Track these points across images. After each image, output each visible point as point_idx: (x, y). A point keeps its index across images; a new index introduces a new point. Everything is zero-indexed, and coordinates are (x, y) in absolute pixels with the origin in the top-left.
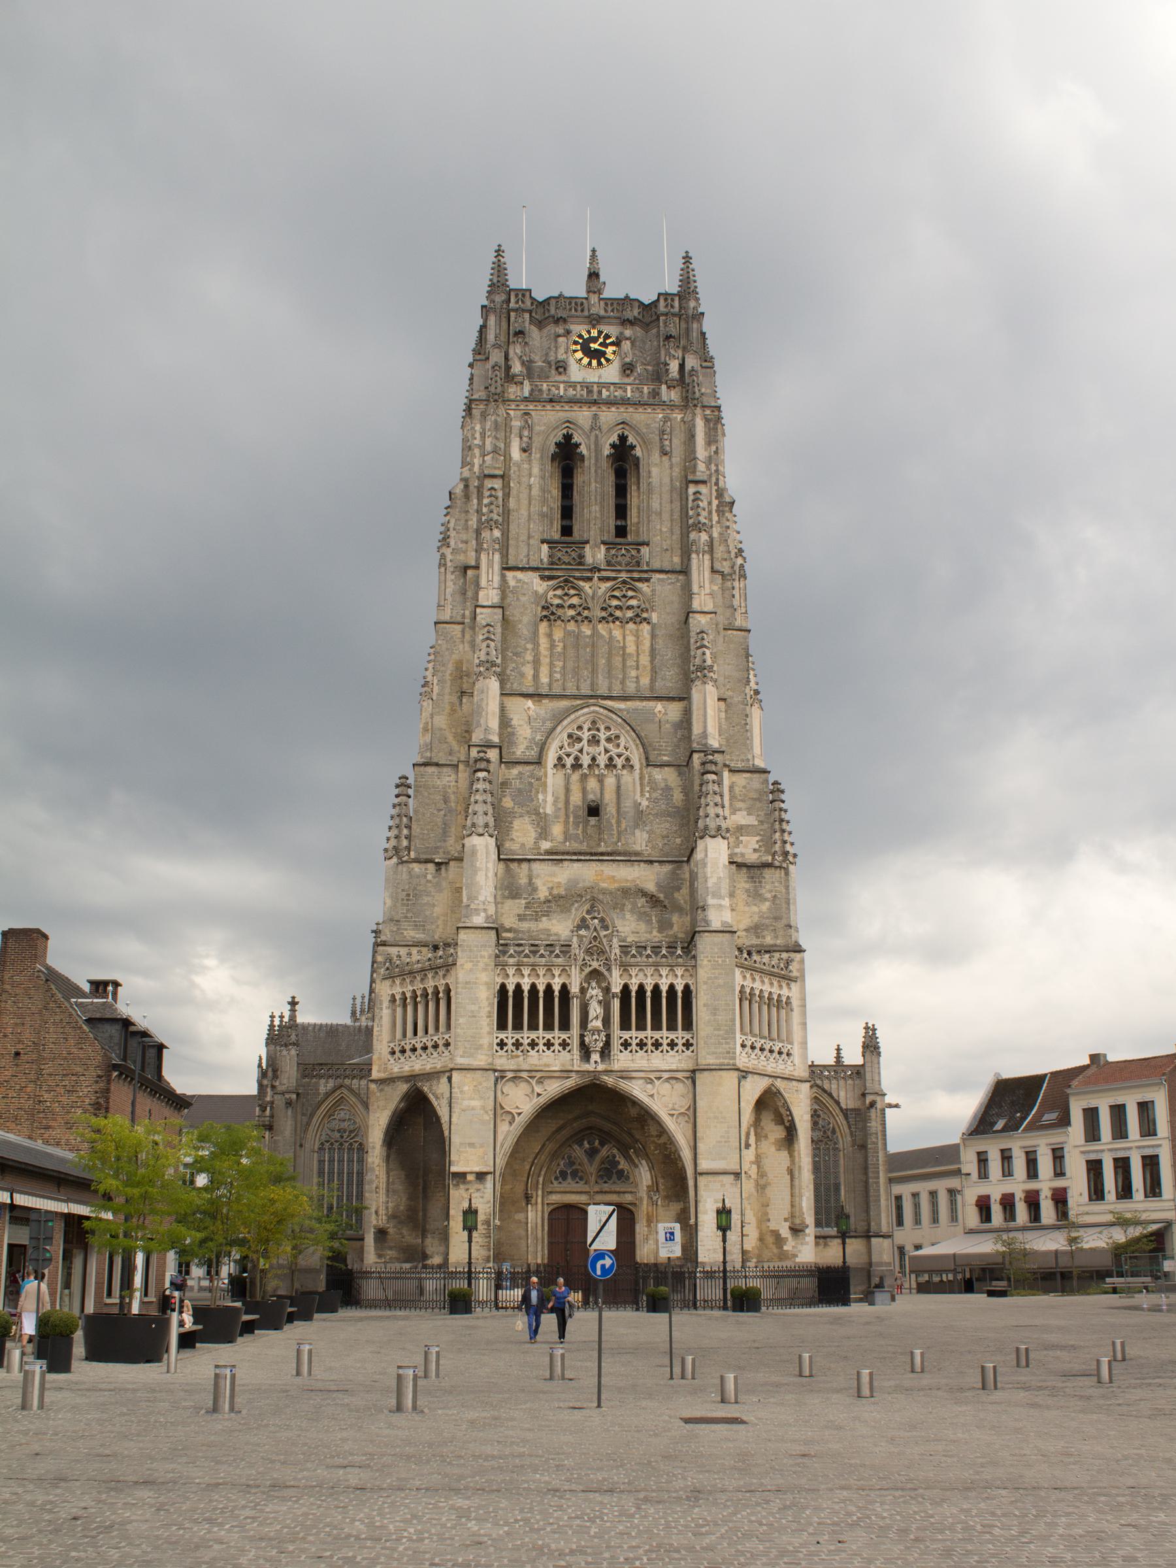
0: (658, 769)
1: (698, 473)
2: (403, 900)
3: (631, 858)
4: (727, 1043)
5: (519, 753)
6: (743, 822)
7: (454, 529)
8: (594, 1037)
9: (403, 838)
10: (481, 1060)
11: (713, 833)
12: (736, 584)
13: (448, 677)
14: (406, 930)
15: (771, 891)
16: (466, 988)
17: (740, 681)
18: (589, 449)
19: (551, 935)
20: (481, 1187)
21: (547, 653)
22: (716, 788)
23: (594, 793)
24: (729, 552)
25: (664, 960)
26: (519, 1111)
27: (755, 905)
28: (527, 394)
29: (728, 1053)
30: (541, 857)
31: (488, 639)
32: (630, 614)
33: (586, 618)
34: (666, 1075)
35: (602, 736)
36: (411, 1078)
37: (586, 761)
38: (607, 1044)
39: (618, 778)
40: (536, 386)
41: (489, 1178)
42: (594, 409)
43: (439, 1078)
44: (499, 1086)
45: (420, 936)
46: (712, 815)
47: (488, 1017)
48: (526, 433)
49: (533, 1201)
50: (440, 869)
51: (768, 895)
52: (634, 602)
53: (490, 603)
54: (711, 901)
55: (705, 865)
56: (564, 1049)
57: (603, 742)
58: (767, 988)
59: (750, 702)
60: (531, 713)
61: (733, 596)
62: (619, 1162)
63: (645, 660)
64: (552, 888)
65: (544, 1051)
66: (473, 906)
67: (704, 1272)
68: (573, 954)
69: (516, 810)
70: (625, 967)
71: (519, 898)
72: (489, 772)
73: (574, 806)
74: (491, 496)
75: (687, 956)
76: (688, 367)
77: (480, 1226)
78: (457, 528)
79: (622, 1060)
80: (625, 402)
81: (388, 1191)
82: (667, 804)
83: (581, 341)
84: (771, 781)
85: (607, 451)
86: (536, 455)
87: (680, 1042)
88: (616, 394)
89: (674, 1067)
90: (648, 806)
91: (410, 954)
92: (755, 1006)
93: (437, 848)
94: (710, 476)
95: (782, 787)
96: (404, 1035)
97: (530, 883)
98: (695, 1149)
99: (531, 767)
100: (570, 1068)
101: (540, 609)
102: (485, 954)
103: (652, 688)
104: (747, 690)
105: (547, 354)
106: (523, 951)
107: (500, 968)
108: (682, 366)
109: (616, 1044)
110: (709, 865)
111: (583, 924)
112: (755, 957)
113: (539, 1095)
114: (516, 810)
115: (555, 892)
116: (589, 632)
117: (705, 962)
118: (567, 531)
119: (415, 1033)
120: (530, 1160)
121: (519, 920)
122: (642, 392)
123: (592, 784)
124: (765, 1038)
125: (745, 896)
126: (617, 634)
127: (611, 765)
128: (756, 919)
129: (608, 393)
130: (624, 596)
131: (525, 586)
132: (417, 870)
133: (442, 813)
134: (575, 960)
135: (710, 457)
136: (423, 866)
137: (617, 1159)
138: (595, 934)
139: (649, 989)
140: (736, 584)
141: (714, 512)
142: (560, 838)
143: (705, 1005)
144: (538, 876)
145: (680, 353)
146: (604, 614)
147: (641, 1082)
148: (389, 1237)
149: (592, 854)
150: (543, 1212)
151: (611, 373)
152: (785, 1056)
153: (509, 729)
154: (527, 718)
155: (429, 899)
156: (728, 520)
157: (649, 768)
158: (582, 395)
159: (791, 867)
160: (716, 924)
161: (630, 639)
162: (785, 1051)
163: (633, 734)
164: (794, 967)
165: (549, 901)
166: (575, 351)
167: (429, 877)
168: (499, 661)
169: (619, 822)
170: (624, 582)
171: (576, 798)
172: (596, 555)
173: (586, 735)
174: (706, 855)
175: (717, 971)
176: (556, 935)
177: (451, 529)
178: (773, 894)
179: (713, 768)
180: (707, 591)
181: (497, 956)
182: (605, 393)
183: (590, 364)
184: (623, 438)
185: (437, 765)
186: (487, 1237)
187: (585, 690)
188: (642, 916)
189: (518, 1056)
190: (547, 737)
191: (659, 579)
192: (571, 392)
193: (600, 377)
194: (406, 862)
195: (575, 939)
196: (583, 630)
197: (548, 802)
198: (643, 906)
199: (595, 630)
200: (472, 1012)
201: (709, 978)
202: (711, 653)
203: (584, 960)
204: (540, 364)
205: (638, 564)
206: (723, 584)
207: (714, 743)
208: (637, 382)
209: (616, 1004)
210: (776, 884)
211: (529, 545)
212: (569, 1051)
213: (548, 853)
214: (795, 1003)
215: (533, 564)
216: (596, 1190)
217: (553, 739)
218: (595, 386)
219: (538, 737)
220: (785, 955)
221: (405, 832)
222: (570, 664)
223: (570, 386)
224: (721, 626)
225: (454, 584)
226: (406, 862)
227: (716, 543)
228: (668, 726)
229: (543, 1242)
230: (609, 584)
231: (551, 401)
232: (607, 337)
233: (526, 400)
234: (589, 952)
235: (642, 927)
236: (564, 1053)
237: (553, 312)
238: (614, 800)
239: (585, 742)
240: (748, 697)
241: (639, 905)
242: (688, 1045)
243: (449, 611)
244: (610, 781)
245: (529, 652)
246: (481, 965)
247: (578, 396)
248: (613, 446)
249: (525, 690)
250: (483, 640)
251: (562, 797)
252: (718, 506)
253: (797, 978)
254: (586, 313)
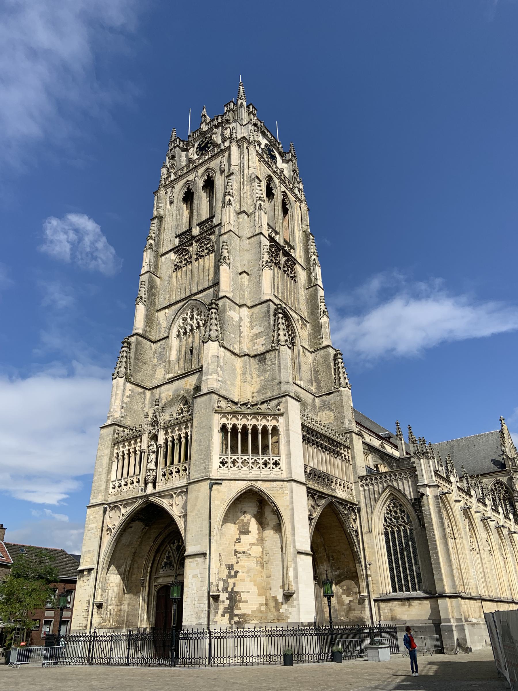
4: (205, 463)
17: (256, 260)
27: (262, 376)
67: (184, 634)
109: (160, 477)
128: (263, 383)
210: (273, 360)
214: (282, 430)
246: (106, 445)
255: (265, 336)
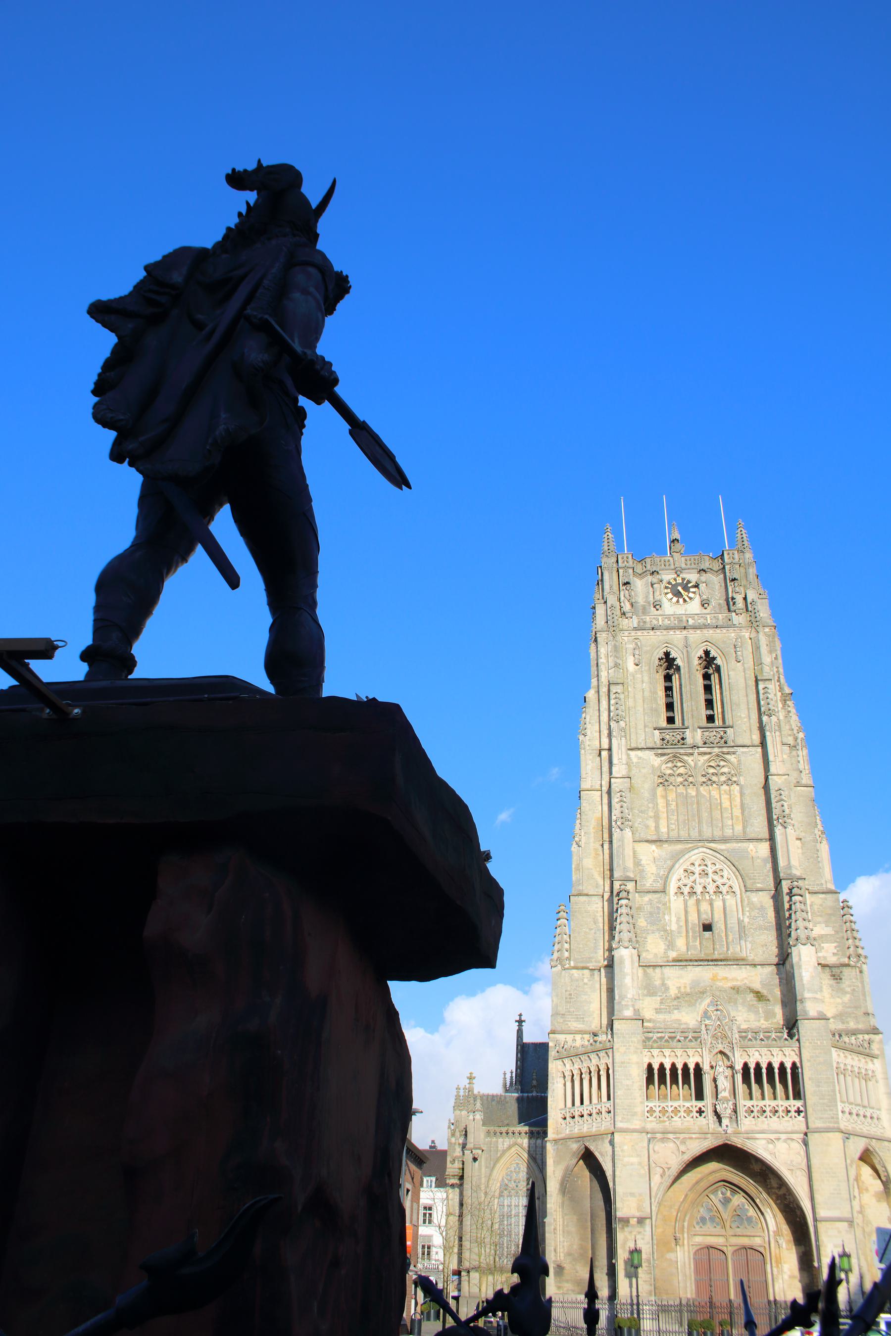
0: (754, 894)
1: (764, 674)
2: (566, 998)
3: (739, 961)
4: (831, 1110)
5: (648, 885)
6: (823, 933)
7: (590, 723)
8: (724, 1105)
9: (565, 950)
10: (636, 1124)
11: (803, 942)
12: (800, 753)
13: (592, 831)
14: (570, 1021)
15: (850, 986)
16: (621, 1067)
18: (683, 661)
19: (681, 1024)
20: (641, 1230)
21: (665, 810)
22: (802, 907)
23: (706, 913)
24: (793, 730)
25: (774, 1042)
26: (669, 1166)
27: (839, 997)
28: (636, 626)
29: (833, 1118)
30: (670, 964)
31: (621, 801)
32: (723, 778)
33: (691, 783)
34: (783, 1136)
35: (710, 870)
36: (580, 1138)
37: (699, 889)
38: (735, 1111)
39: (724, 901)
40: (642, 619)
41: (648, 1221)
42: (685, 632)
43: (603, 1138)
44: (651, 1146)
45: (580, 1026)
46: (801, 928)
47: (640, 1090)
48: (637, 652)
49: (681, 1242)
50: (594, 974)
51: (848, 989)
52: (725, 770)
53: (621, 776)
54: (807, 995)
55: (800, 967)
56: (700, 1115)
57: (711, 875)
58: (855, 1063)
59: (819, 839)
60: (656, 855)
61: (799, 762)
62: (747, 1210)
63: (737, 812)
64: (680, 987)
65: (684, 1117)
66: (623, 1003)
68: (702, 1039)
69: (648, 928)
70: (744, 1048)
71: (656, 996)
72: (629, 900)
73: (692, 924)
74: (616, 698)
75: (791, 1039)
76: (749, 600)
77: (643, 1265)
78: (592, 722)
79: (747, 1123)
80: (706, 626)
81: (564, 1232)
82: (764, 920)
83: (670, 586)
84: (841, 900)
85: (696, 662)
86: (645, 668)
87: (793, 1109)
88: (699, 621)
89: (789, 1129)
90: (749, 922)
91: (574, 1040)
92: (849, 1079)
93: (589, 958)
94: (774, 675)
95: (850, 904)
96: (573, 1104)
97: (663, 984)
98: (812, 1199)
99: (657, 895)
100: (706, 1131)
101: (656, 777)
102: (635, 1040)
103: (744, 832)
104: (816, 831)
105: (647, 597)
106: (664, 1037)
107: (647, 1050)
108: (745, 599)
109: (742, 1111)
110: (803, 967)
111: (706, 1015)
112: (846, 1039)
113: (683, 1153)
114: (648, 928)
115: (683, 990)
116: (694, 794)
117: (807, 1044)
118: (671, 720)
119: (582, 1103)
120: (677, 1207)
121: (657, 1013)
122: (718, 619)
123: (704, 906)
124: (859, 1105)
125: (830, 991)
126: (715, 793)
127: (718, 892)
128: (840, 1008)
129: (693, 621)
130: (719, 766)
131: (645, 762)
132: (576, 975)
133: (593, 931)
134: (705, 1044)
135: (772, 662)
136: (580, 972)
137: (746, 1207)
138: (719, 1023)
139: (764, 1066)
140: (800, 753)
141: (779, 701)
142: (683, 948)
143: (810, 1079)
144: (669, 978)
145: (742, 588)
146: (704, 779)
147: (764, 1142)
148: (565, 1271)
149: (708, 961)
150: (689, 1252)
151: (694, 606)
152: (875, 1120)
153: (640, 867)
154: (652, 860)
155: (586, 997)
156: (789, 706)
157: (748, 893)
158: (675, 624)
159: (864, 966)
160: (812, 1013)
161: (725, 797)
162: (875, 1116)
163: (733, 867)
164: (875, 1046)
165: (678, 998)
166: (666, 594)
167: (586, 981)
168: (630, 817)
169: (726, 936)
170: (718, 755)
171: (693, 918)
172: (694, 736)
173: (697, 870)
174: (800, 959)
175: (817, 1051)
176: (686, 1024)
177: (587, 723)
178: (852, 988)
179: (799, 892)
180: (780, 759)
181: (644, 1041)
182: (691, 622)
183: (678, 601)
184: (707, 653)
185: (587, 895)
186: (649, 1273)
187: (694, 834)
188: (751, 1008)
189: (664, 1121)
190: (669, 873)
191: (743, 752)
192: (667, 622)
193: (686, 610)
194: (567, 969)
195: (703, 1027)
196: (689, 792)
197: (673, 921)
198: (751, 1000)
199: (698, 790)
200: (627, 1085)
201: (811, 1057)
202: (788, 805)
203: (711, 1043)
204: (642, 603)
205: (726, 743)
206: (791, 753)
207: (797, 872)
208: (713, 612)
209: (739, 1078)
210: (854, 980)
211: (645, 731)
212: (705, 1117)
213: (674, 961)
215: (651, 745)
216: (731, 1233)
217: (673, 874)
218: (684, 616)
219: (662, 873)
220: (866, 1037)
221: (567, 946)
222: (681, 818)
223: (666, 618)
224: (792, 785)
225: (592, 762)
226: (567, 969)
227: (782, 724)
228: (759, 861)
229: (691, 1279)
230: (707, 757)
231: (653, 629)
232: (689, 582)
233: (635, 629)
234: (714, 1036)
235: (752, 1016)
236: (701, 1119)
237: (648, 567)
238: (723, 919)
239: (697, 875)
240: (818, 838)
241: (748, 1000)
242: (799, 1112)
243: (590, 782)
244: (718, 904)
245: (650, 810)
247: (673, 625)
248: (700, 658)
249: (650, 838)
250: (617, 803)
251: (683, 918)
252: (781, 697)
253: (878, 1055)
254: (672, 567)
255: (837, 942)
